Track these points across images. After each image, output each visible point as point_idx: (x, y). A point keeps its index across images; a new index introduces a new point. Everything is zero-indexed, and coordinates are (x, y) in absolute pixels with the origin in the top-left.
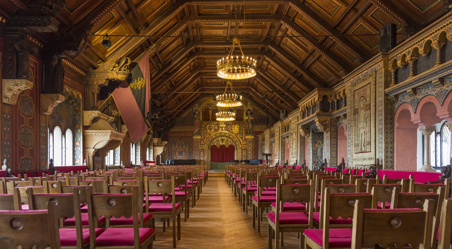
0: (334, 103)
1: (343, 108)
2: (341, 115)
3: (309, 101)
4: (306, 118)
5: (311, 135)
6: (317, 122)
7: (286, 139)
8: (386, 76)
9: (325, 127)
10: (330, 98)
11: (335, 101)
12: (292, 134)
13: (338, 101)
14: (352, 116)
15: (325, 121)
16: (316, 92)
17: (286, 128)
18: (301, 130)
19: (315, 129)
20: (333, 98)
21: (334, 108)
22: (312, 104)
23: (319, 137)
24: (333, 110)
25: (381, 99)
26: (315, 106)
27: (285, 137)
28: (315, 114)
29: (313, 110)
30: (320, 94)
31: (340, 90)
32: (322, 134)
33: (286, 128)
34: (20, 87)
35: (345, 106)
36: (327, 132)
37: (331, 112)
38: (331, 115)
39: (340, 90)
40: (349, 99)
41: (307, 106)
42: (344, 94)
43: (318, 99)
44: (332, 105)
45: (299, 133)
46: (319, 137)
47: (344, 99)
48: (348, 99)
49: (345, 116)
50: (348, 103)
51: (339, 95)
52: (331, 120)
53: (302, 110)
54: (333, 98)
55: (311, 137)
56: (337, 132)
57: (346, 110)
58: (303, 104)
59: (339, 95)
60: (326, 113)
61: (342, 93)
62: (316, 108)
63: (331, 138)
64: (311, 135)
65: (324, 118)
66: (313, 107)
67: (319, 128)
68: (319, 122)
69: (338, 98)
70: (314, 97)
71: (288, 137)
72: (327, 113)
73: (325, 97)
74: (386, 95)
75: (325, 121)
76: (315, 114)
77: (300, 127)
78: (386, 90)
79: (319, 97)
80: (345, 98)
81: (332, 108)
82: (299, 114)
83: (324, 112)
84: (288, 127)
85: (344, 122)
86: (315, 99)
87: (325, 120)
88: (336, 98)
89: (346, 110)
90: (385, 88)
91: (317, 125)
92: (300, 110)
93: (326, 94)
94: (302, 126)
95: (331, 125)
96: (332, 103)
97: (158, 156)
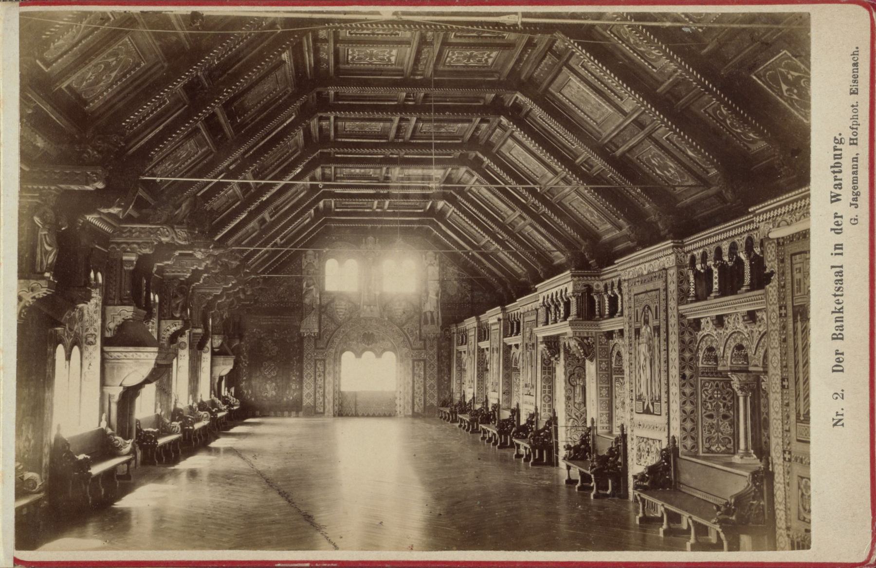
3: (561, 287)
8: (681, 282)
15: (587, 338)
17: (512, 324)
25: (673, 321)
34: (36, 294)
42: (620, 290)
51: (612, 289)
55: (562, 361)
61: (616, 285)
70: (566, 286)
74: (681, 316)
75: (587, 338)
78: (681, 307)
86: (566, 290)
90: (679, 304)
97: (221, 378)
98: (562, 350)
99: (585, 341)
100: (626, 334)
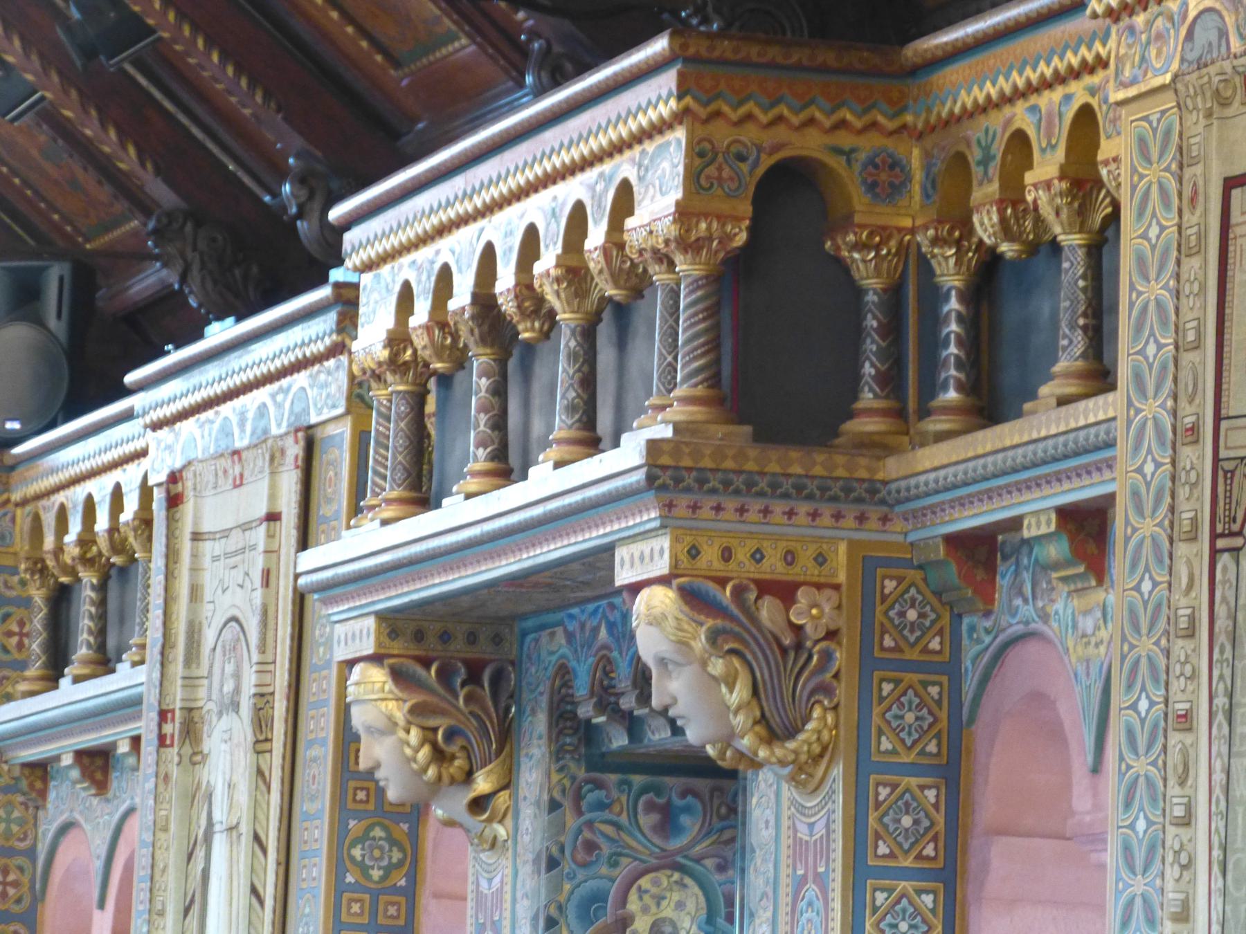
0: (932, 295)
1: (1043, 423)
2: (1037, 511)
3: (534, 209)
4: (459, 513)
5: (533, 775)
6: (660, 599)
7: (67, 798)
9: (782, 678)
10: (860, 200)
11: (950, 273)
12: (191, 730)
13: (988, 274)
14: (1193, 555)
16: (658, 96)
17: (61, 598)
18: (375, 696)
19: (605, 697)
20: (911, 214)
21: (929, 387)
22: (574, 272)
23: (668, 822)
24: (907, 412)
26: (622, 312)
27: (41, 770)
28: (626, 457)
29: (588, 382)
30: (722, 134)
31: (1020, 116)
32: (709, 787)
33: (61, 598)
35: (1100, 376)
36: (804, 772)
37: (878, 447)
38: (873, 498)
39: (1020, 116)
40: (1157, 290)
41: (484, 300)
42: (1083, 181)
43: (683, 213)
44: (893, 329)
45: (320, 727)
46: (668, 822)
47: (1074, 267)
48: (1139, 291)
49: (1088, 527)
50: (1131, 352)
51: (1012, 196)
52: (869, 566)
53: (398, 339)
54: (911, 214)
55: (527, 826)
56: (952, 770)
57: (1096, 449)
58: (428, 241)
59: (1012, 196)
60: (794, 462)
61: (1046, 167)
62: (650, 353)
63: (859, 871)
64: (533, 775)
65: (768, 538)
66: (588, 334)
67: (675, 689)
68: (693, 598)
69: (985, 225)
70: (624, 167)
71: (98, 765)
72: (819, 463)
73: (789, 193)
75: (785, 592)
76: (626, 457)
77: (350, 632)
79: (693, 179)
80: (1102, 245)
81: (891, 381)
82: (321, 396)
83: (766, 435)
84: (117, 571)
85: (1074, 630)
87: (773, 566)
88: (958, 223)
89: (1096, 449)
91: (650, 644)
92: (371, 337)
93: (811, 145)
94: (391, 622)
95: (867, 662)
96: (894, 295)
98: (537, 724)
99: (768, 611)
100: (1133, 529)
